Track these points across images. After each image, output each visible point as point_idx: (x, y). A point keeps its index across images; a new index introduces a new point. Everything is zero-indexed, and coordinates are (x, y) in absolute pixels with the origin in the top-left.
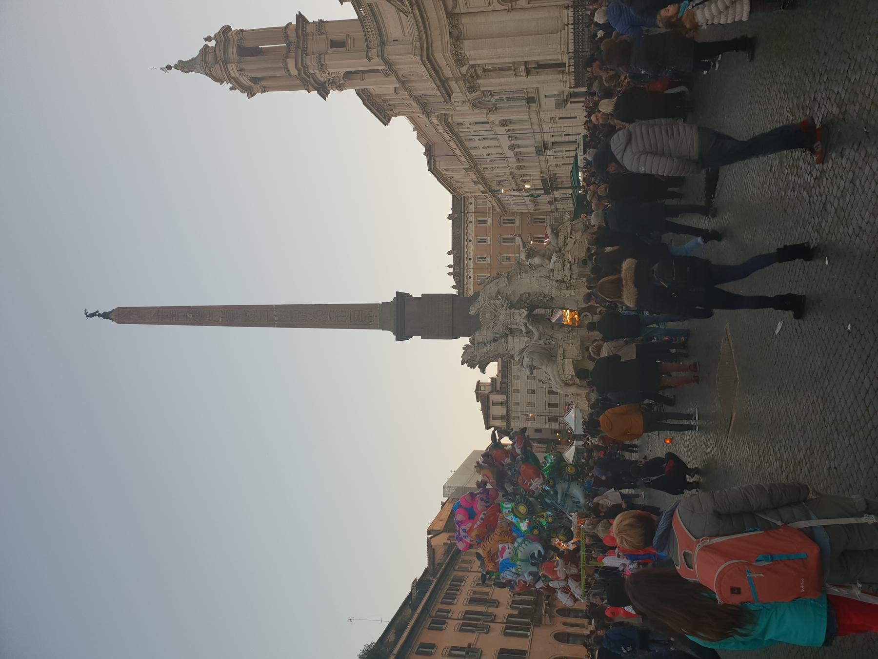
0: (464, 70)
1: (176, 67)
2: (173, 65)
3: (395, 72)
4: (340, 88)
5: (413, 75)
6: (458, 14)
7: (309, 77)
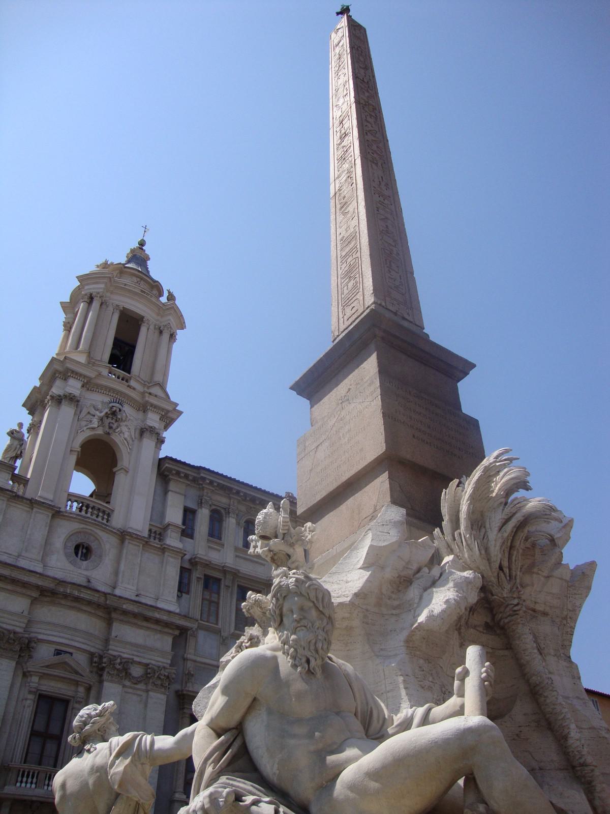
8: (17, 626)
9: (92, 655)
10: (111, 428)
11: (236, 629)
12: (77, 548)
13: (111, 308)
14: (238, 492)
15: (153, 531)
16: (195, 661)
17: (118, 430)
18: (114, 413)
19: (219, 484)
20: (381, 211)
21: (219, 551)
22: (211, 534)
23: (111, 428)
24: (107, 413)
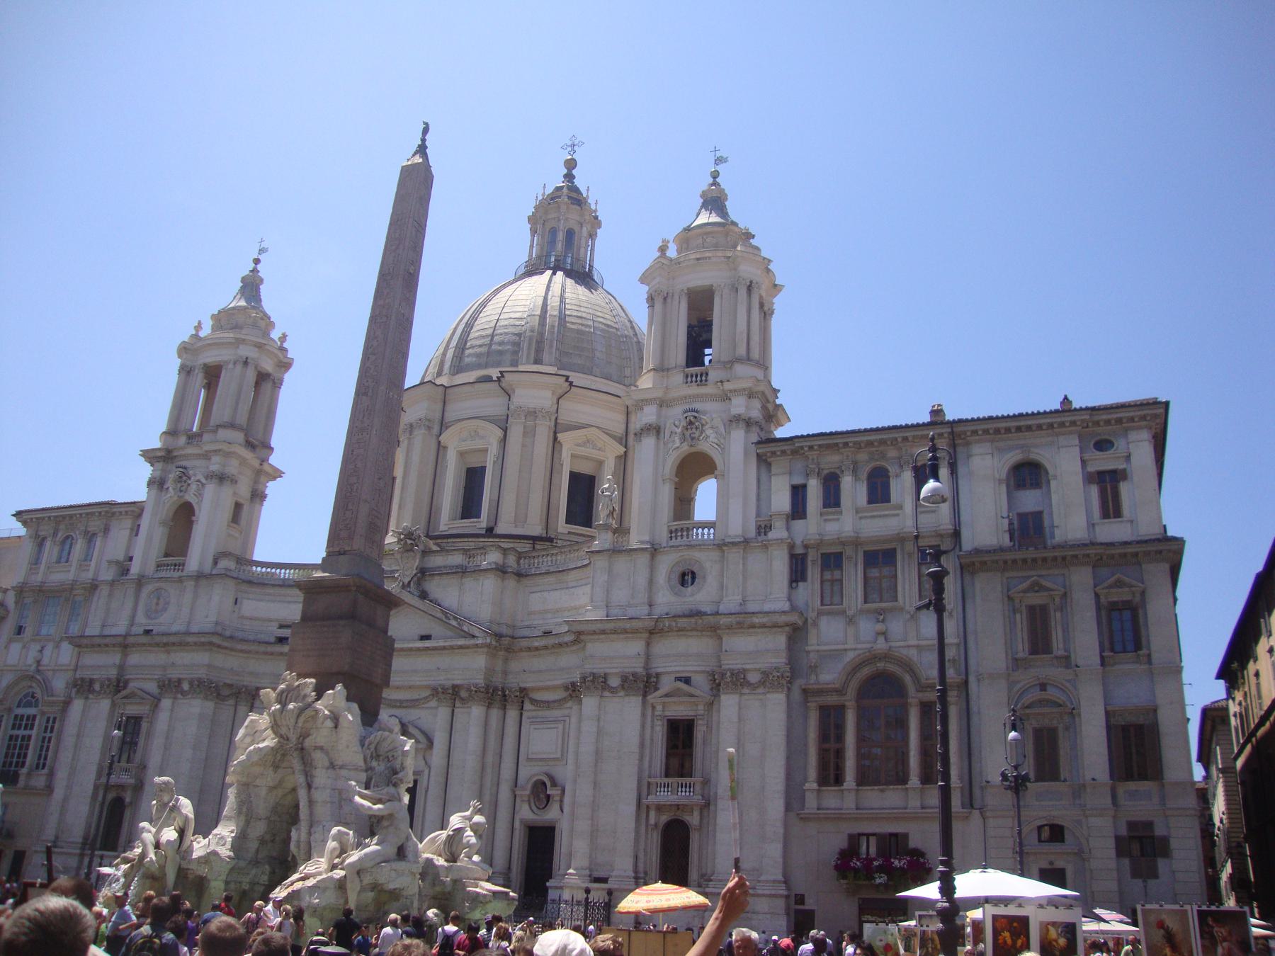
0: (152, 687)
1: (254, 271)
2: (259, 267)
3: (180, 580)
4: (157, 484)
5: (157, 604)
6: (253, 703)
7: (210, 451)
8: (638, 666)
9: (708, 672)
10: (693, 439)
11: (866, 602)
12: (684, 575)
13: (676, 297)
14: (846, 444)
15: (763, 526)
16: (818, 651)
17: (704, 435)
18: (691, 423)
19: (820, 446)
20: (355, 453)
21: (838, 519)
22: (827, 504)
23: (693, 439)
24: (684, 427)
